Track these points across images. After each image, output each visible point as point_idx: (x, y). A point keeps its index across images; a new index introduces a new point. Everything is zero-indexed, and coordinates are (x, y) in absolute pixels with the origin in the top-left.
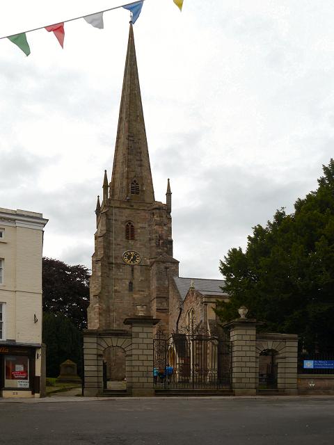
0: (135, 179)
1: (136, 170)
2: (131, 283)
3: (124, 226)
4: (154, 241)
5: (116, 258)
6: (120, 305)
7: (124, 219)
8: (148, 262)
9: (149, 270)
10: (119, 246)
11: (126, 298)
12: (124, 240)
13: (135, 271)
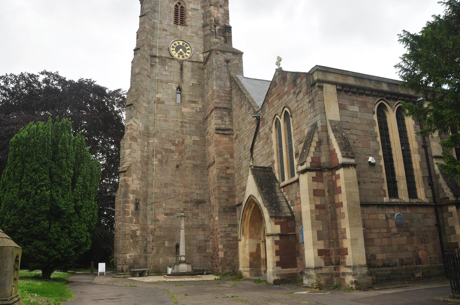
2: (179, 89)
3: (173, 6)
4: (208, 28)
5: (160, 49)
6: (164, 125)
8: (201, 58)
9: (203, 69)
10: (164, 32)
11: (173, 113)
12: (172, 23)
13: (185, 70)
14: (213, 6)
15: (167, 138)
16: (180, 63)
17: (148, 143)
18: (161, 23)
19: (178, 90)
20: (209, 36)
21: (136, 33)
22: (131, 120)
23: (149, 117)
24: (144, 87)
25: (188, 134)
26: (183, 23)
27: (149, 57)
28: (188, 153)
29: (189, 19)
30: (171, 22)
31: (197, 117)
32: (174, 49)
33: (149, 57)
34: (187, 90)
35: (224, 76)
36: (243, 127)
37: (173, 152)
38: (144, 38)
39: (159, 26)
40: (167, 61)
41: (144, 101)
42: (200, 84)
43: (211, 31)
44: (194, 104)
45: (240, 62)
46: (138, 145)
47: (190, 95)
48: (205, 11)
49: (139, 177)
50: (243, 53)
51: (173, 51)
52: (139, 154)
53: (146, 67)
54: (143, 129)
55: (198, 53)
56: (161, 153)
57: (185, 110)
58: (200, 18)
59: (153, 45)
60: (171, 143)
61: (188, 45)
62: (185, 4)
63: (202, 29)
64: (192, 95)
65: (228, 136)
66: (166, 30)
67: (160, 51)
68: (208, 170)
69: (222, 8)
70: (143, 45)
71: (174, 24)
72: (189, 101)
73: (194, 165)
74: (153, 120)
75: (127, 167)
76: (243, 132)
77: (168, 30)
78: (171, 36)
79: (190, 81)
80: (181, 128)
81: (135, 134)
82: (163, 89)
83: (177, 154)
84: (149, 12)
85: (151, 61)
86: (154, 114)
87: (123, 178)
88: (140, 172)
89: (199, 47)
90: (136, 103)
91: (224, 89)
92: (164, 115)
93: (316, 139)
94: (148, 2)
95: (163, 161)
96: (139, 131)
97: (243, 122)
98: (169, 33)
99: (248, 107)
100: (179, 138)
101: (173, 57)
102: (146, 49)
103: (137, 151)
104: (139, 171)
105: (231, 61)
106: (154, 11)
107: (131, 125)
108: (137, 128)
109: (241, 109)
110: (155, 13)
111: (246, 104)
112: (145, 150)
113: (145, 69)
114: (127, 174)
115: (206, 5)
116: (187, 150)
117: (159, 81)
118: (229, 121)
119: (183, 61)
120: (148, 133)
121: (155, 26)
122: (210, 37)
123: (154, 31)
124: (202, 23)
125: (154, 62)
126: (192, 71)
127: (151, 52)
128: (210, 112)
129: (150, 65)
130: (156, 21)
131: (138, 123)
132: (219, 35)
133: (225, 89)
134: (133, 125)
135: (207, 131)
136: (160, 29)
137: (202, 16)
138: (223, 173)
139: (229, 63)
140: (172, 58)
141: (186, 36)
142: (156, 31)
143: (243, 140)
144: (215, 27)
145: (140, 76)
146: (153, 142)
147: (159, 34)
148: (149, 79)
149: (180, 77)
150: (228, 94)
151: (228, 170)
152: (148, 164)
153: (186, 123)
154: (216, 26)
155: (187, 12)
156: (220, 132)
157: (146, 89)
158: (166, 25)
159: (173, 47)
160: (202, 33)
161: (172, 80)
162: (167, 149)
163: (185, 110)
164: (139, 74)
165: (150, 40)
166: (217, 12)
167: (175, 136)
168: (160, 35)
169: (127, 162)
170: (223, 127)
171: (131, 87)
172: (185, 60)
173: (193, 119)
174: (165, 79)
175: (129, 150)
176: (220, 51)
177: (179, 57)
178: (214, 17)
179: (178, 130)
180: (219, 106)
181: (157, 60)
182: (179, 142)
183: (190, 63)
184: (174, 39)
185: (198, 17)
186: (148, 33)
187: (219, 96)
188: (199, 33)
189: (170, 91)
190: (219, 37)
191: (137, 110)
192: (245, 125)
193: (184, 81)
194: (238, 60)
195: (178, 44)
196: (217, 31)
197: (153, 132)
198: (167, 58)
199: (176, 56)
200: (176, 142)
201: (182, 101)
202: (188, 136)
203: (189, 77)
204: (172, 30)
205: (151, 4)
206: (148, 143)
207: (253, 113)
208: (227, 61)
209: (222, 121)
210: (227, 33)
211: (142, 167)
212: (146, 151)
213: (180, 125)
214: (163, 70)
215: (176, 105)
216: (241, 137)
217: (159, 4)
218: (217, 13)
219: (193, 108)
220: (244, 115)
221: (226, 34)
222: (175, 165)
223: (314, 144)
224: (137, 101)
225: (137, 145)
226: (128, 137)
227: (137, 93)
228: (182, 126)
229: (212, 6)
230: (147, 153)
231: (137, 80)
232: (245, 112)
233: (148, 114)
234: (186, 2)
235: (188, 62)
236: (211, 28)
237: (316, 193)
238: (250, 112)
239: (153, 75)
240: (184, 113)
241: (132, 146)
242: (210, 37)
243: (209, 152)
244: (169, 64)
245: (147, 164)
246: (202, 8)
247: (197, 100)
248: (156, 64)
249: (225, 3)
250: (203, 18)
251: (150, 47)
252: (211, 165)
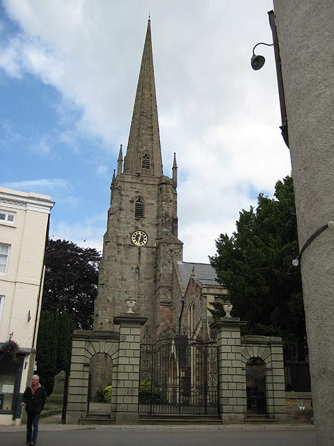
0: (146, 152)
13: (142, 254)
93: (200, 326)
223: (199, 329)
237: (197, 356)
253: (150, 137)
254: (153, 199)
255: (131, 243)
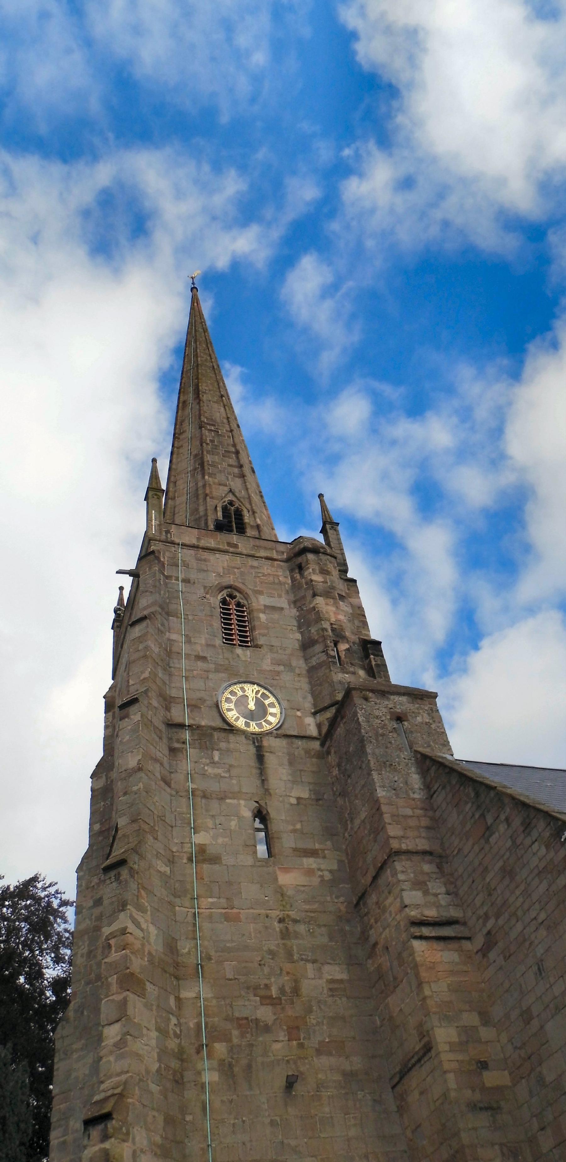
0: (230, 497)
1: (232, 483)
3: (216, 600)
4: (318, 648)
5: (194, 707)
7: (213, 579)
10: (200, 664)
12: (218, 641)
13: (271, 760)
14: (321, 596)
15: (242, 979)
16: (254, 743)
17: (178, 999)
18: (189, 641)
19: (257, 820)
20: (323, 668)
21: (104, 697)
22: (122, 915)
23: (177, 908)
24: (156, 812)
25: (307, 961)
26: (247, 642)
27: (164, 726)
28: (317, 1028)
29: (262, 631)
30: (216, 638)
31: (329, 899)
32: (232, 706)
33: (162, 727)
34: (283, 818)
35: (398, 756)
36: (511, 900)
37: (267, 1029)
38: (146, 675)
39: (185, 649)
40: (216, 738)
41: (158, 855)
42: (320, 800)
43: (327, 654)
44: (311, 860)
45: (433, 718)
46: (148, 1006)
47: (295, 831)
48: (302, 610)
49: (158, 1139)
50: (437, 693)
51: (229, 710)
52: (153, 1043)
53: (159, 755)
54: (160, 948)
55: (299, 714)
56: (226, 1038)
57: (286, 879)
58: (289, 628)
59: (173, 695)
60: (255, 995)
61: (270, 695)
62: (246, 597)
63: (301, 654)
64: (302, 833)
65: (454, 945)
66: (204, 659)
67: (191, 711)
68: (398, 1088)
69: (346, 600)
70: (146, 692)
71: (224, 643)
72: (295, 850)
73: (345, 1074)
74: (190, 918)
75: (116, 1098)
76: (520, 913)
77: (209, 658)
78: (218, 672)
79: (291, 792)
80: (283, 939)
81: (137, 964)
82: (213, 816)
83: (282, 1036)
84: (156, 611)
85: (170, 739)
86: (189, 896)
87: (96, 1148)
88: (160, 1119)
89: (301, 699)
90: (136, 859)
91: (409, 795)
92: (223, 901)
94: (151, 590)
95: (236, 1069)
96: (150, 953)
97: (507, 881)
98: (212, 666)
99: (522, 824)
100: (281, 974)
101: (233, 726)
102: (155, 703)
103: (145, 1031)
104: (156, 1114)
105: (410, 718)
106: (168, 614)
107: (124, 931)
108: (143, 945)
109: (487, 841)
110: (171, 618)
111: (507, 820)
112: (171, 1026)
113: (156, 760)
114: (114, 1128)
115: (304, 597)
116: (312, 1020)
117: (198, 793)
118: (448, 893)
119: (262, 735)
120: (177, 965)
121: (175, 649)
122: (328, 670)
123: (171, 662)
124: (298, 640)
125: (178, 741)
126: (291, 763)
127: (168, 714)
128: (372, 872)
129: (167, 748)
130: (174, 637)
131: (144, 926)
132: (352, 664)
133: (412, 795)
134: (130, 931)
135: (372, 940)
136: (188, 656)
137: (296, 624)
138: (473, 1091)
139: (406, 723)
140: (230, 729)
141: (261, 672)
142: (176, 661)
143: (527, 944)
144: (336, 645)
145: (143, 775)
146: (194, 995)
147: (188, 668)
148: (168, 789)
149: (259, 782)
150: (422, 809)
151: (485, 1074)
152: (183, 1083)
153: (295, 921)
154: (338, 642)
155: (255, 614)
156: (426, 931)
157: (162, 818)
158: (201, 645)
159: (228, 700)
160: (301, 663)
161: (236, 789)
162: (247, 1018)
163: (286, 879)
164: (140, 769)
165: (164, 683)
166: (334, 609)
167: (266, 970)
168: (189, 670)
169: (110, 1077)
170: (431, 913)
171: (90, 845)
172: (267, 734)
173: (315, 906)
174: (214, 787)
175: (116, 1027)
176: (372, 691)
177: (247, 724)
178: (329, 621)
179: (273, 948)
180: (404, 847)
181: (187, 735)
182: (282, 990)
183: (284, 742)
184: (229, 681)
185: (284, 627)
186: (157, 663)
187: (398, 816)
188: (294, 663)
189: (233, 824)
190: (352, 669)
191: (140, 881)
192: (522, 887)
193: (271, 791)
194: (429, 714)
195: (240, 693)
196: (342, 655)
197: (192, 961)
198: (215, 729)
199: (241, 723)
200: (274, 992)
201: (276, 850)
202: (309, 966)
203: (285, 778)
204: (221, 657)
205: (160, 594)
206: (178, 999)
207: (548, 834)
208: (399, 719)
209: (426, 893)
210: (372, 656)
211: (166, 1098)
212: (175, 1033)
213: (278, 929)
214: (208, 761)
215: (258, 864)
216: (514, 934)
217: (178, 597)
218: (335, 613)
219: (310, 872)
220: (505, 857)
221: (370, 661)
222: (280, 1082)
224: (137, 853)
225: (146, 1005)
226: (113, 980)
227: (135, 826)
228: (285, 934)
229: (318, 596)
230: (177, 1041)
231: (135, 788)
232: (509, 843)
233: (171, 898)
234: (250, 593)
235: (276, 737)
236: (326, 646)
238: (535, 834)
239: (178, 777)
240: (285, 889)
241: (130, 1012)
242: (328, 670)
243: (391, 1018)
244: (223, 745)
245: (179, 1082)
246: (292, 606)
247: (317, 846)
248: (184, 746)
249: (349, 589)
250: (299, 627)
251: (165, 699)
252: (414, 1065)
253: (236, 470)
254: (280, 596)
255: (219, 723)
